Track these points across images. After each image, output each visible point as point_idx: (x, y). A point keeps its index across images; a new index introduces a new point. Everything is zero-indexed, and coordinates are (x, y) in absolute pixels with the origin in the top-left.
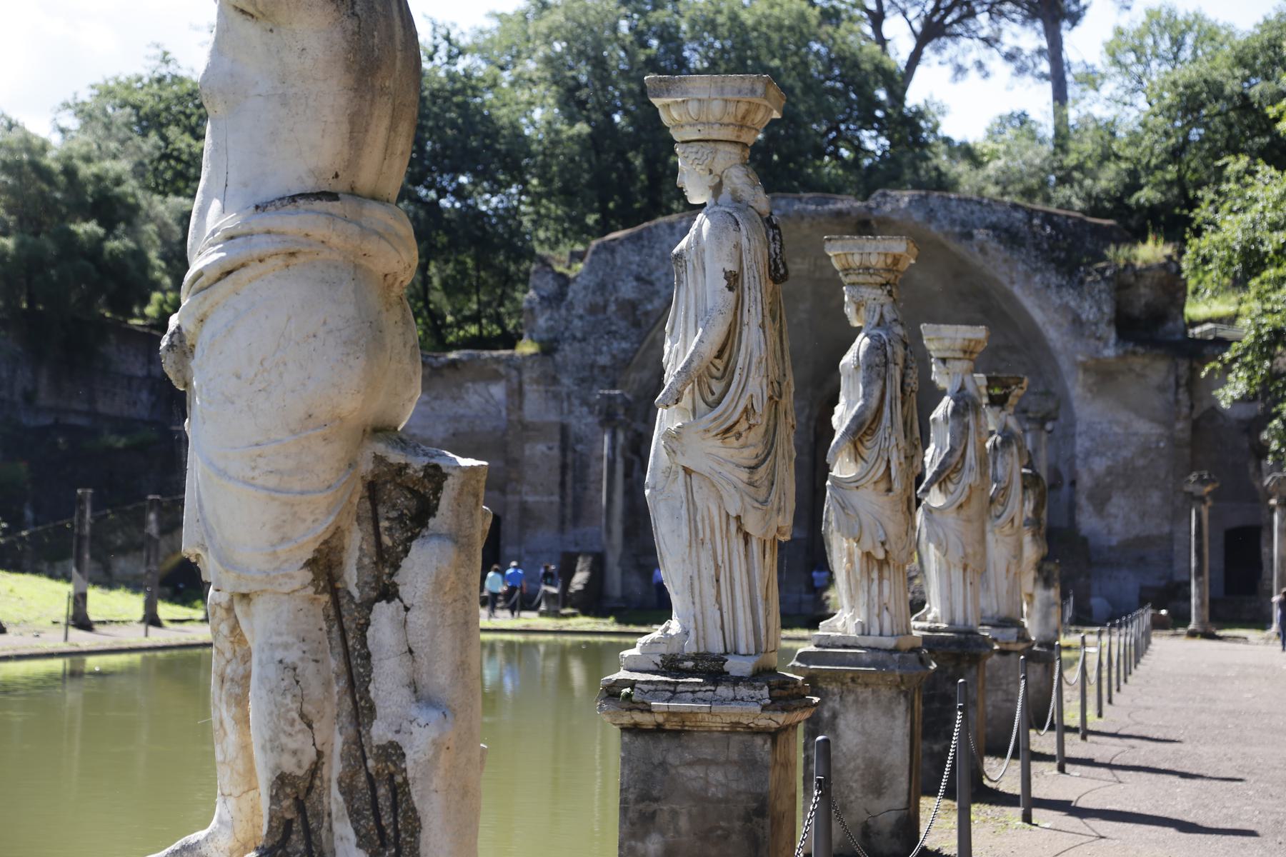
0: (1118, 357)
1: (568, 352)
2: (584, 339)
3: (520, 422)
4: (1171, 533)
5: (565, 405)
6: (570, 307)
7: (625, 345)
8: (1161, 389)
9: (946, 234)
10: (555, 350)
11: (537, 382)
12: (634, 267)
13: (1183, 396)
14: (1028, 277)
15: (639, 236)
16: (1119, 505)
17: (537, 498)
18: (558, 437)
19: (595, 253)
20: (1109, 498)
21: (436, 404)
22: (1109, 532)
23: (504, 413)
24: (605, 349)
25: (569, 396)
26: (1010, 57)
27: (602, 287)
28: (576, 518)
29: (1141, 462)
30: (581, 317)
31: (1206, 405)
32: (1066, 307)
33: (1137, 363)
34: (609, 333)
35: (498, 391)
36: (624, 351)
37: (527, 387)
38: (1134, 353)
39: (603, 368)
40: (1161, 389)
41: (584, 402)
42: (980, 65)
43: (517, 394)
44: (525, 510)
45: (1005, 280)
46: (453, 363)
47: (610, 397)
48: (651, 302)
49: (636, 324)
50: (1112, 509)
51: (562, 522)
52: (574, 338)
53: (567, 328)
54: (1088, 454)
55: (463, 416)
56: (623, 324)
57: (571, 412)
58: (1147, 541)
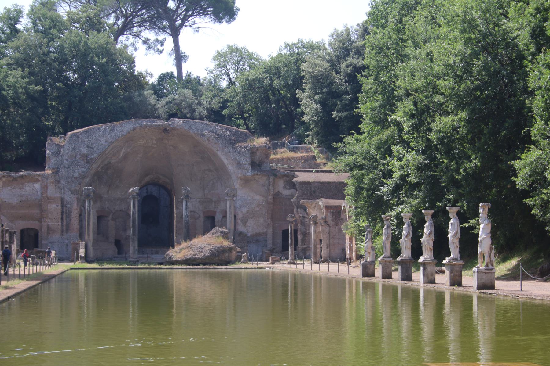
0: (252, 175)
1: (63, 171)
2: (69, 168)
3: (47, 197)
4: (266, 232)
5: (62, 191)
6: (62, 156)
7: (84, 170)
8: (263, 185)
9: (196, 134)
10: (59, 171)
11: (53, 183)
12: (86, 143)
13: (271, 188)
14: (223, 149)
15: (87, 131)
16: (251, 223)
17: (53, 223)
18: (60, 202)
19: (71, 137)
20: (247, 221)
21: (14, 190)
22: (248, 232)
23: (39, 194)
24: (76, 171)
25: (64, 188)
26: (145, 42)
27: (74, 149)
28: (67, 230)
29: (257, 209)
30: (67, 160)
31: (276, 190)
32: (235, 159)
33: (257, 177)
34: (78, 165)
35: (37, 186)
36: (84, 172)
37: (48, 184)
38: (257, 174)
39: (76, 178)
40: (263, 185)
41: (69, 190)
42: (133, 45)
43: (45, 188)
44: (49, 228)
45: (215, 150)
46: (22, 176)
47: (88, 189)
48: (93, 155)
49: (88, 162)
50: (248, 224)
51: (62, 232)
52: (65, 167)
53: (62, 164)
54: (241, 207)
55: (23, 195)
56: (82, 162)
57: (64, 193)
58: (259, 234)
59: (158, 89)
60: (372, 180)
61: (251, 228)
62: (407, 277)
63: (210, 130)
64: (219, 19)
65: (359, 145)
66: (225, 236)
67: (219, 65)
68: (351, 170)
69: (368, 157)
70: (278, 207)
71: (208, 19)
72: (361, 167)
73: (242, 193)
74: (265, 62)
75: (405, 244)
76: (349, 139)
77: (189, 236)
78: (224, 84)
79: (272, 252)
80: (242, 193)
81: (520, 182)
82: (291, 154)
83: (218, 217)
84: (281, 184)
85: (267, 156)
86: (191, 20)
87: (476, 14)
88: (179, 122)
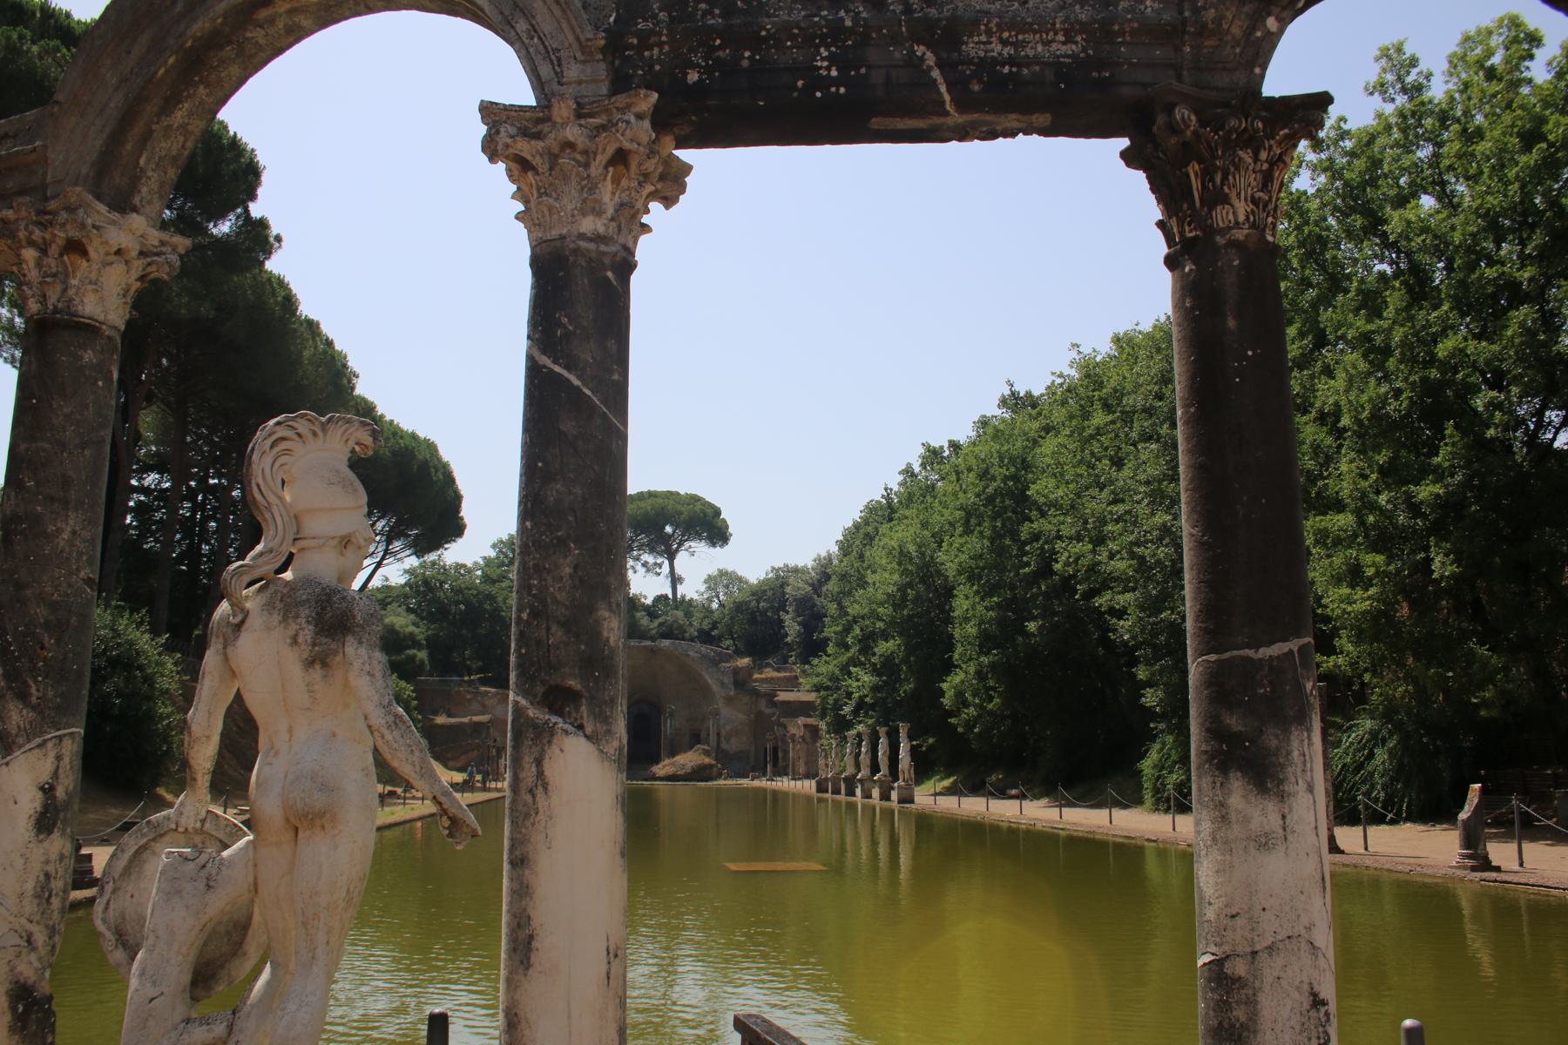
16: (734, 740)
26: (645, 565)
59: (651, 612)
60: (836, 701)
61: (733, 745)
62: (885, 796)
63: (696, 651)
64: (714, 545)
65: (825, 666)
66: (707, 753)
67: (709, 588)
68: (818, 691)
69: (834, 678)
70: (760, 724)
71: (703, 543)
72: (827, 688)
73: (726, 712)
74: (751, 586)
75: (865, 758)
76: (816, 661)
77: (673, 754)
78: (715, 606)
79: (754, 769)
80: (726, 712)
81: (946, 701)
82: (776, 674)
83: (703, 735)
84: (763, 703)
85: (751, 675)
86: (687, 544)
87: (912, 548)
88: (666, 643)
